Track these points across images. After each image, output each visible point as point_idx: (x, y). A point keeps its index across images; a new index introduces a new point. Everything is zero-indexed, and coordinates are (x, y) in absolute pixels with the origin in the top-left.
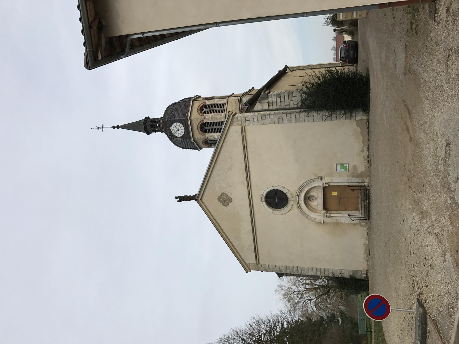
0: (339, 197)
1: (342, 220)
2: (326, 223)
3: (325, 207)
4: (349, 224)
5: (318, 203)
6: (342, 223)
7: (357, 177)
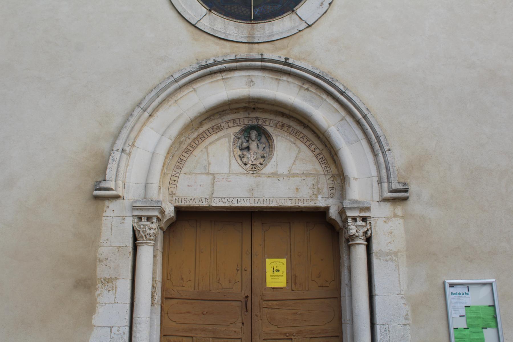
0: (252, 301)
3: (188, 217)
6: (91, 310)
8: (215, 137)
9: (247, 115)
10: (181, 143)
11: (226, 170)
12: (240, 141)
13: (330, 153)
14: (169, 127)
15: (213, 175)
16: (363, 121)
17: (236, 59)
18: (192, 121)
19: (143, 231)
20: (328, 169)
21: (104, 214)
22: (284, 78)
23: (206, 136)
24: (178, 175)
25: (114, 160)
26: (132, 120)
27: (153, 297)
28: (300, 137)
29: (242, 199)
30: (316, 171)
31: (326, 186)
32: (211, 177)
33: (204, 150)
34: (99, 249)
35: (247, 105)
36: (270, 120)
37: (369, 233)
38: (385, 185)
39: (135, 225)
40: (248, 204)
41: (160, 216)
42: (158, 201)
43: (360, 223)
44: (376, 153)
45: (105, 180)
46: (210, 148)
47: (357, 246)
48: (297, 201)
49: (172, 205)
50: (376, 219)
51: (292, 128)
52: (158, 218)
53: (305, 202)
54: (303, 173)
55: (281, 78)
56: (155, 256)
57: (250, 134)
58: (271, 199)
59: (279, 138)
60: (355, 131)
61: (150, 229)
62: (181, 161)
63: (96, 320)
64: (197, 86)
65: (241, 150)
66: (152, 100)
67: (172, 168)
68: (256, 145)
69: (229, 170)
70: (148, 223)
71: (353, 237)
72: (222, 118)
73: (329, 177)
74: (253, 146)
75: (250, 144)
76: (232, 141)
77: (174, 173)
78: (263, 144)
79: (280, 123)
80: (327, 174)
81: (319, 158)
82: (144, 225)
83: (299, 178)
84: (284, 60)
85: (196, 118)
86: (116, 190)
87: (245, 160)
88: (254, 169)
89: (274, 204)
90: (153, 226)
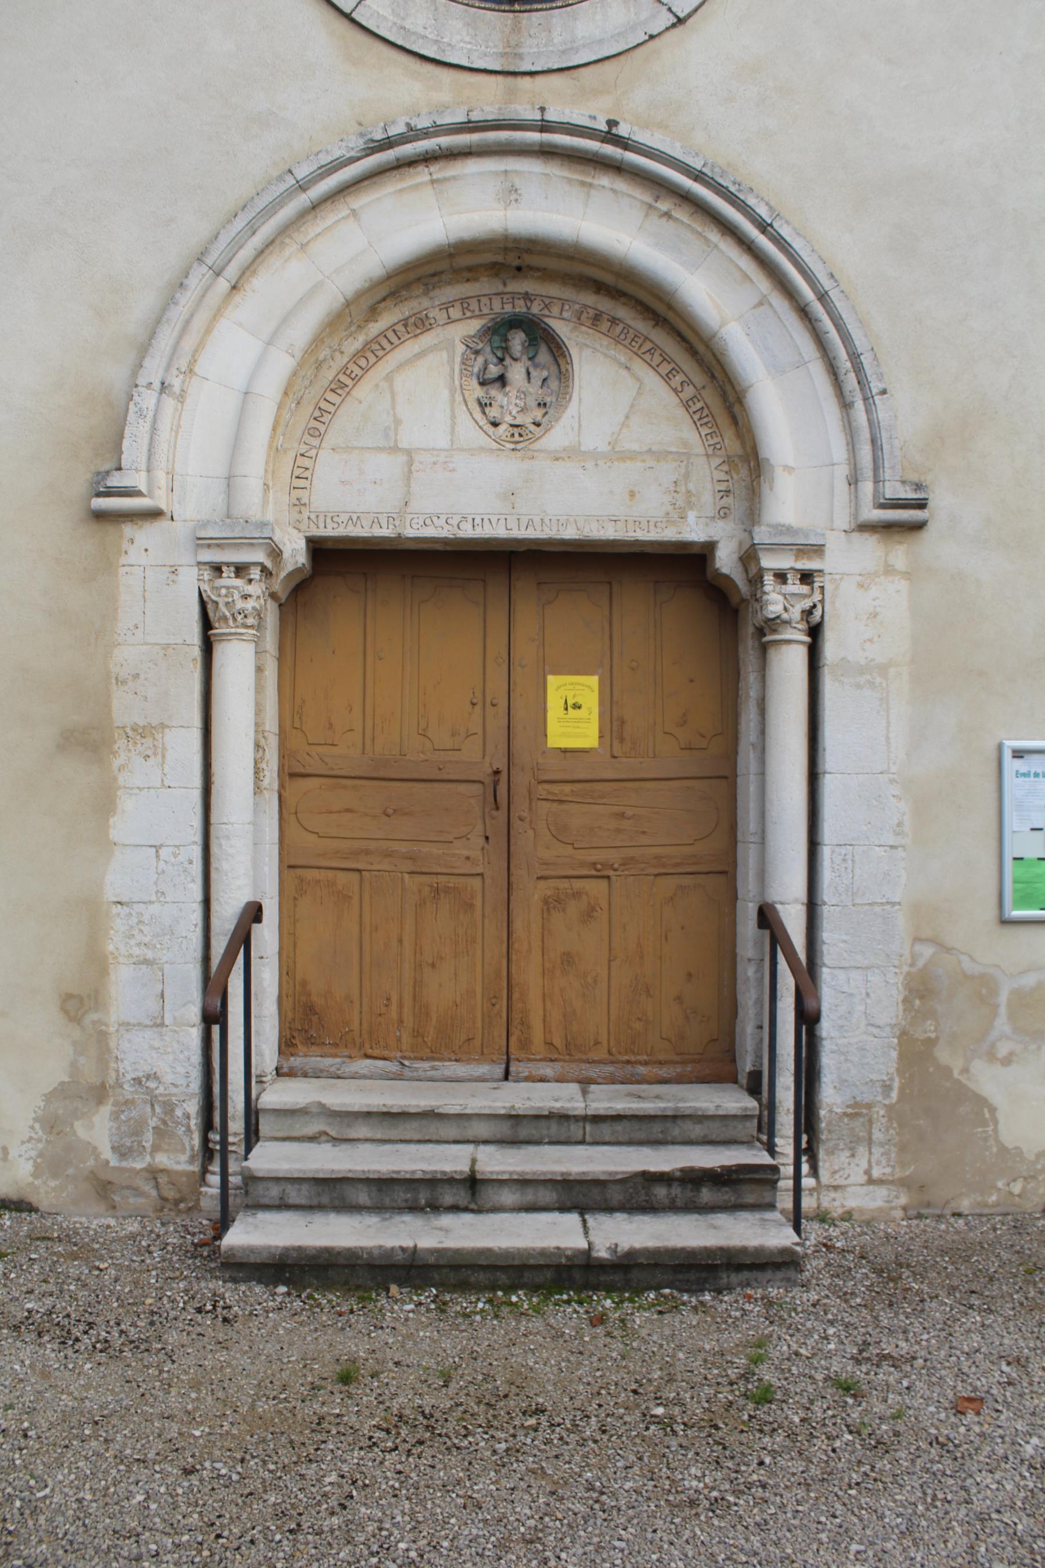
1: (154, 803)
2: (107, 564)
3: (342, 566)
4: (92, 913)
5: (436, 456)
6: (105, 804)
7: (915, 1054)
8: (411, 348)
9: (501, 288)
10: (319, 365)
11: (442, 441)
12: (480, 360)
13: (724, 396)
14: (285, 320)
15: (408, 452)
16: (818, 309)
17: (469, 122)
18: (348, 304)
19: (227, 603)
20: (716, 440)
21: (123, 560)
22: (605, 180)
23: (388, 347)
24: (313, 453)
25: (141, 414)
26: (186, 300)
27: (257, 771)
28: (643, 350)
29: (486, 517)
30: (685, 444)
31: (709, 485)
32: (402, 458)
33: (384, 385)
34: (116, 651)
35: (499, 259)
36: (564, 301)
37: (817, 613)
38: (867, 488)
39: (205, 587)
40: (500, 532)
41: (269, 564)
42: (263, 525)
43: (795, 587)
44: (848, 399)
45: (120, 469)
46: (399, 381)
47: (784, 648)
48: (630, 526)
49: (301, 535)
50: (837, 577)
51: (621, 326)
52: (264, 569)
53: (652, 528)
54: (650, 451)
55: (596, 182)
56: (259, 669)
57: (506, 340)
58: (563, 519)
59: (587, 352)
60: (795, 336)
61: (245, 597)
62: (320, 415)
63: (119, 829)
64: (361, 200)
65: (482, 384)
66: (237, 244)
67: (300, 432)
68: (524, 370)
69: (452, 441)
70: (239, 582)
71: (774, 624)
72: (431, 294)
73: (718, 461)
74: (516, 373)
75: (506, 367)
76: (458, 359)
77: (303, 448)
78: (544, 367)
79: (590, 311)
80: (714, 455)
81: (694, 408)
82: (228, 588)
83: (639, 464)
84: (604, 128)
85: (360, 295)
86: (150, 495)
87: (493, 412)
88: (517, 438)
89: (569, 533)
90: (251, 589)
